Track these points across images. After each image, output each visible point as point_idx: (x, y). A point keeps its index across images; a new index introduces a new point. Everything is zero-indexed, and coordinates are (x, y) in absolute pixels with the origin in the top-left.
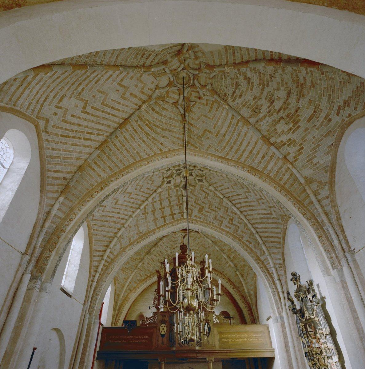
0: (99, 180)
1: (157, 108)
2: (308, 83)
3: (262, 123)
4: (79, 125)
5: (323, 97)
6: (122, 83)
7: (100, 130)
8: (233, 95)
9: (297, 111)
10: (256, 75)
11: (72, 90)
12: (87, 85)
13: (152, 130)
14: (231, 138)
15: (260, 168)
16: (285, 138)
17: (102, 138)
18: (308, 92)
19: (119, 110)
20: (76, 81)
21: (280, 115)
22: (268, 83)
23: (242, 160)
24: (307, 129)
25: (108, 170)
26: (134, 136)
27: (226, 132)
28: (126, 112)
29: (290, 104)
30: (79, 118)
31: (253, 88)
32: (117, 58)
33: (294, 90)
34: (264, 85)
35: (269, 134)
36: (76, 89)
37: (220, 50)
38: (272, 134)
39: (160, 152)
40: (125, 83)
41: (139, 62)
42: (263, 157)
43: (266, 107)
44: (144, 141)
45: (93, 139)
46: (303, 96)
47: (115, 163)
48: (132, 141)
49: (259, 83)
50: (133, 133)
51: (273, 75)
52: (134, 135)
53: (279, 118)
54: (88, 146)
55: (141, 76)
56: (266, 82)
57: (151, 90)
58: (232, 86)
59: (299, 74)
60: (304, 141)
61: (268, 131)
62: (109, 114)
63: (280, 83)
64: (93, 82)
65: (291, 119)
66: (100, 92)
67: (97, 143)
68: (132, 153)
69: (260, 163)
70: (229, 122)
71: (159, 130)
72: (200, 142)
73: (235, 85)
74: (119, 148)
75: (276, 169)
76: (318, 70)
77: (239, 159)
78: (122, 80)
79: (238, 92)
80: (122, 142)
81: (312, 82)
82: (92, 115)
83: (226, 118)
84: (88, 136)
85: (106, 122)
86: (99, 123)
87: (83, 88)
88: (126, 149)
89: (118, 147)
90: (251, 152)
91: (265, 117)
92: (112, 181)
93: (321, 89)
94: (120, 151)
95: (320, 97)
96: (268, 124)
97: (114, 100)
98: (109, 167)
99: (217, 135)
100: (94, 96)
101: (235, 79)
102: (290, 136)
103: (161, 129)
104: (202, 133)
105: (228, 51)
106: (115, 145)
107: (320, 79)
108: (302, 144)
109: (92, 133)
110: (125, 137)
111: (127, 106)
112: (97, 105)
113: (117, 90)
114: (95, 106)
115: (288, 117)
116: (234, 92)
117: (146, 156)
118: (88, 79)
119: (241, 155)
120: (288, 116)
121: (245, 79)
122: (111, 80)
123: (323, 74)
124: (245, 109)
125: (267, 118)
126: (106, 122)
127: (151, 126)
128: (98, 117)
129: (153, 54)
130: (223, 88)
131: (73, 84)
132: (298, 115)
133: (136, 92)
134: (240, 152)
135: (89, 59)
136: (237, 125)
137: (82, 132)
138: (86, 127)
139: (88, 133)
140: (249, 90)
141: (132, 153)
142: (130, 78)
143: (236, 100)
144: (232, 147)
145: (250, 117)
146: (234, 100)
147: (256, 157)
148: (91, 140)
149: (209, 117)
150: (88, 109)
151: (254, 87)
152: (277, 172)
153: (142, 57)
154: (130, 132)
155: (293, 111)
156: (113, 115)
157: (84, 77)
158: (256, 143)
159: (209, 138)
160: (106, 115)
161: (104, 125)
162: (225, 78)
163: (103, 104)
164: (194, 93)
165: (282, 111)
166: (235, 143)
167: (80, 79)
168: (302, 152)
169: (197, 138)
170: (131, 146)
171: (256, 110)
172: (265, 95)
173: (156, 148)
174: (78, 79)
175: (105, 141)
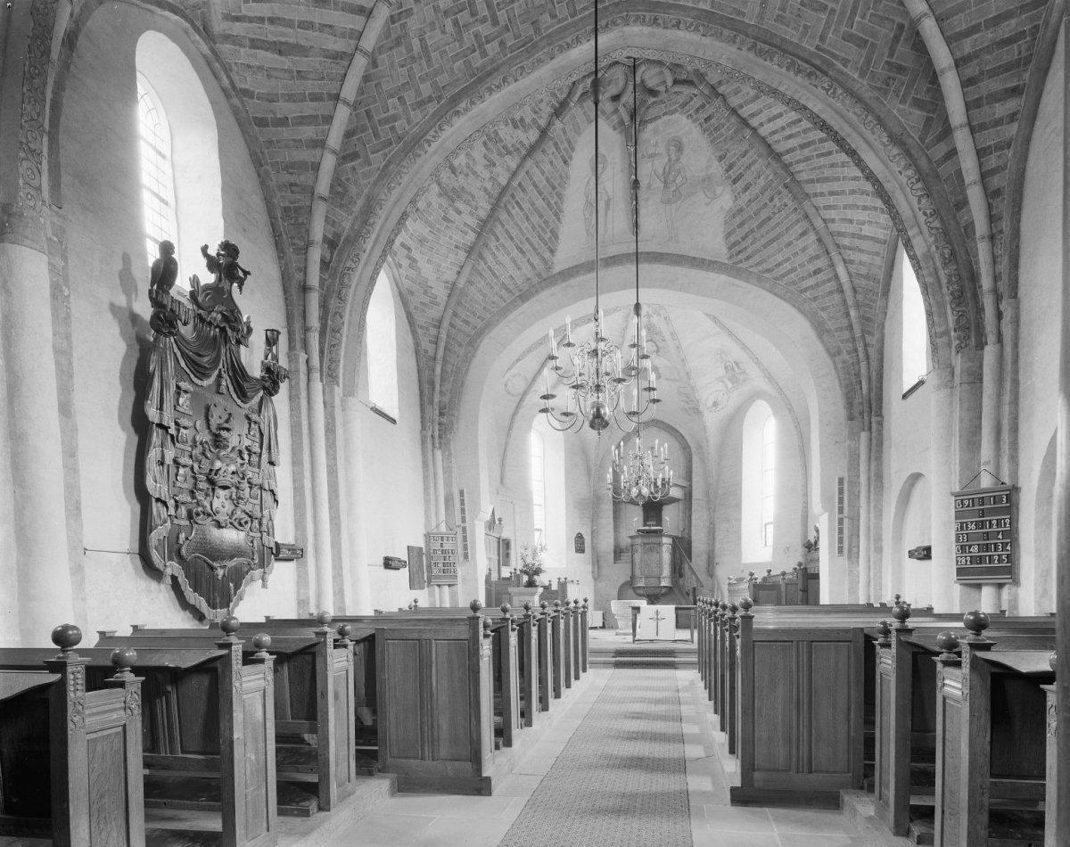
2: (452, 214)
10: (509, 141)
18: (441, 205)
22: (486, 148)
32: (746, 152)
59: (469, 209)
105: (566, 145)
118: (805, 141)
121: (522, 120)
142: (741, 91)
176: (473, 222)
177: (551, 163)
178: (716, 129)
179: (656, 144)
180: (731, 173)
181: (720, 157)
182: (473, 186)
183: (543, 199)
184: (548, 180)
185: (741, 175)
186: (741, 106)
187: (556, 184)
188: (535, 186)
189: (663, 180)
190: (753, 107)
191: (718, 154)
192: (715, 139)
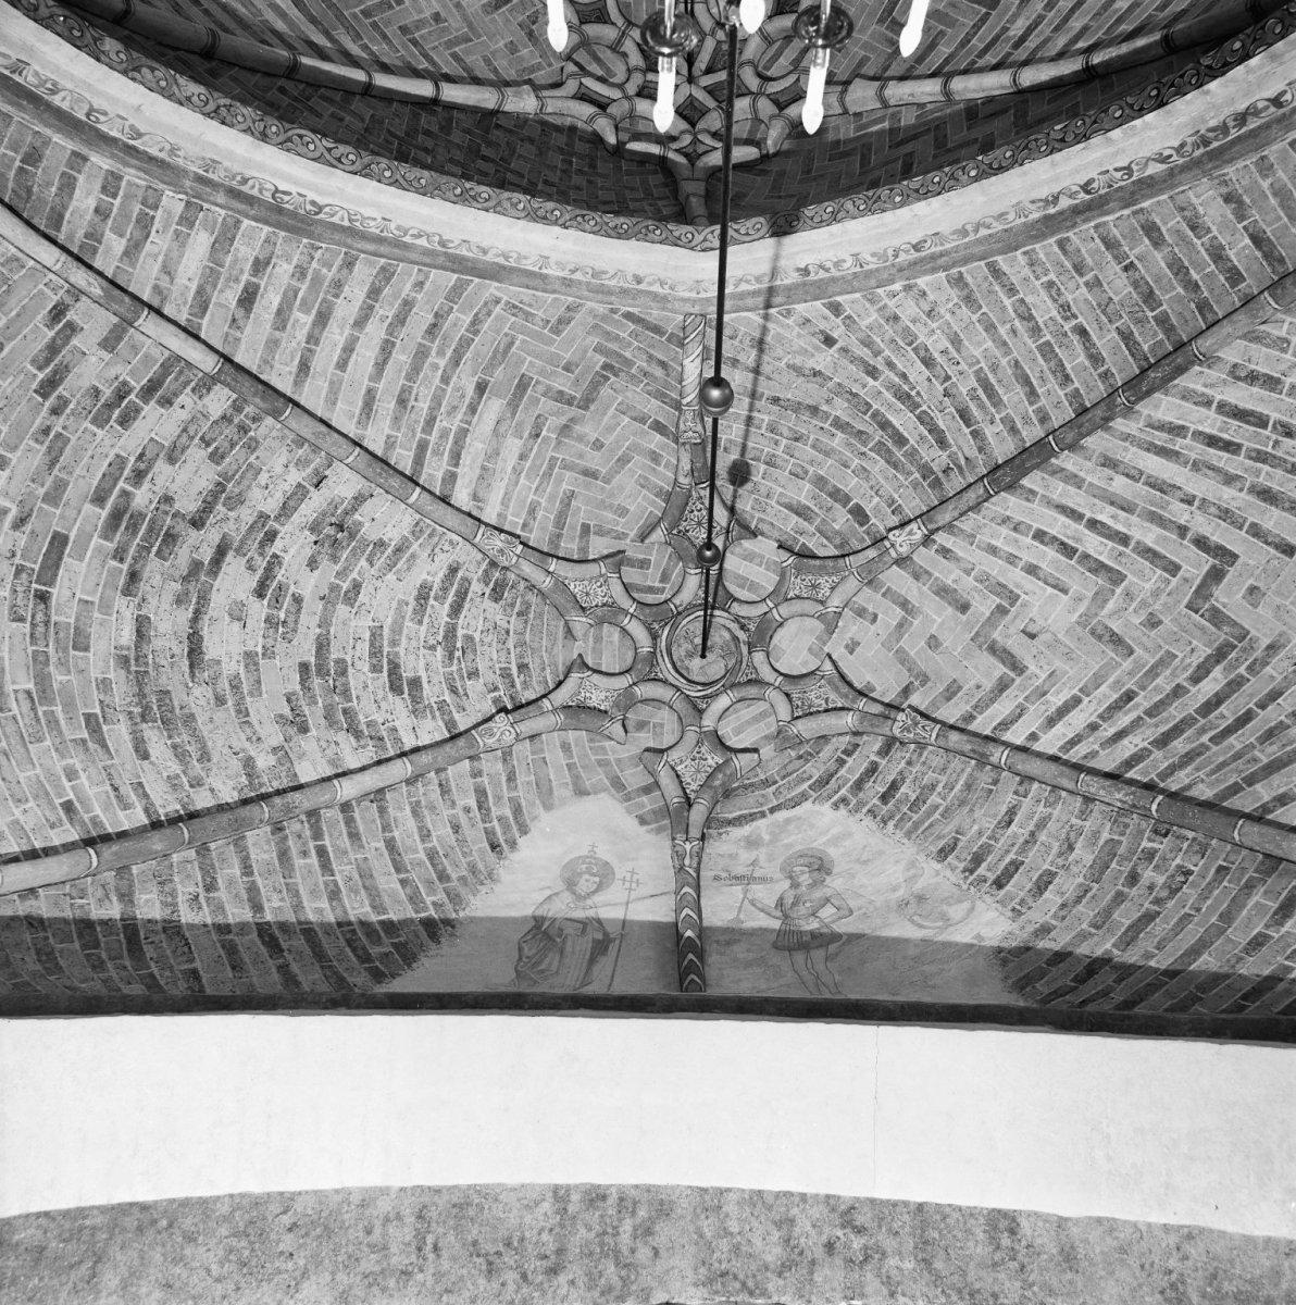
0: (1238, 172)
1: (841, 519)
2: (119, 733)
3: (295, 476)
4: (1267, 495)
5: (31, 686)
6: (1001, 670)
7: (1162, 452)
8: (462, 595)
9: (134, 576)
10: (366, 711)
11: (1256, 688)
12: (1178, 691)
13: (875, 415)
14: (445, 380)
15: (253, 237)
16: (157, 424)
17: (1163, 407)
19: (1040, 536)
20: (1228, 731)
21: (209, 538)
22: (303, 681)
23: (364, 273)
24: (53, 498)
25: (1170, 224)
26: (980, 392)
27: (473, 409)
28: (1005, 520)
29: (179, 601)
30: (1256, 531)
31: (372, 645)
33: (173, 676)
34: (322, 671)
35: (243, 429)
36: (1235, 685)
37: (548, 807)
38: (230, 431)
39: (839, 299)
40: (988, 670)
41: (909, 763)
42: (248, 299)
43: (287, 558)
44: (928, 362)
45: (1212, 413)
46: (124, 661)
47: (1118, 258)
48: (994, 368)
49: (344, 673)
50: (982, 406)
51: (292, 731)
52: (975, 398)
53: (212, 520)
54: (1252, 378)
55: (906, 691)
56: (316, 682)
57: (861, 612)
58: (469, 638)
60: (46, 431)
61: (252, 446)
62: (1093, 524)
63: (251, 694)
64: (1143, 701)
65: (150, 529)
66: (1116, 640)
67: (1192, 386)
68: (1007, 302)
69: (260, 266)
70: (466, 459)
71: (840, 408)
72: (613, 346)
73: (459, 645)
74: (1075, 338)
75: (158, 243)
76: (95, 821)
77: (386, 274)
78: (1002, 686)
79: (440, 611)
80: (1054, 373)
81: (104, 746)
82: (1182, 531)
83: (481, 477)
84: (1235, 431)
85: (1120, 485)
86: (1154, 484)
87: (1196, 679)
88: (1036, 331)
89: (1079, 348)
90: (323, 319)
91: (286, 511)
92: (1163, 159)
93: (53, 722)
94: (1074, 322)
95: (42, 680)
96: (263, 478)
97: (1054, 587)
98: (1158, 241)
99: (523, 385)
100: (1153, 622)
101: (462, 677)
102: (130, 442)
103: (827, 415)
104: (605, 391)
105: (508, 813)
106: (1096, 359)
107: (71, 774)
108: (55, 411)
109: (1212, 441)
110: (1032, 394)
111: (993, 550)
112: (1144, 580)
113: (1032, 636)
114: (1159, 572)
115: (167, 534)
116: (456, 610)
117: (922, 282)
119: (374, 293)
120: (171, 538)
121: (415, 683)
122: (1056, 700)
123: (68, 807)
124: (393, 535)
125: (271, 506)
126: (1120, 485)
127: (878, 435)
128: (1156, 519)
129: (843, 791)
130: (515, 623)
131: (1247, 718)
132: (119, 555)
133: (938, 616)
134: (386, 310)
135: (1145, 844)
136: (422, 447)
137: (1261, 457)
138: (1230, 480)
139: (1230, 447)
140: (386, 631)
141: (1007, 302)
142: (960, 688)
143: (441, 575)
144: (432, 330)
145: (360, 499)
146: (453, 570)
147: (289, 297)
148: (1223, 408)
149: (568, 474)
150: (1196, 565)
151: (364, 648)
152: (145, 223)
153: (894, 786)
154: (997, 417)
155: (153, 568)
156: (1076, 516)
157: (1180, 745)
158: (304, 368)
159: (567, 368)
160: (1110, 522)
161: (1134, 475)
162: (510, 675)
163: (1116, 578)
164: (649, 583)
165: (206, 555)
166: (421, 354)
167: (1205, 739)
168: (40, 368)
169: (629, 363)
170: (1005, 343)
171: (337, 532)
172: (309, 624)
173: (864, 324)
174: (1215, 740)
175: (1140, 386)
176: (166, 805)
177: (456, 828)
178: (914, 806)
179: (754, 863)
180: (981, 870)
181: (941, 850)
182: (221, 733)
183: (403, 882)
184: (432, 855)
185: (1015, 866)
186: (970, 718)
187: (454, 876)
188: (391, 845)
189: (779, 914)
190: (1002, 708)
191: (934, 849)
192: (916, 825)
